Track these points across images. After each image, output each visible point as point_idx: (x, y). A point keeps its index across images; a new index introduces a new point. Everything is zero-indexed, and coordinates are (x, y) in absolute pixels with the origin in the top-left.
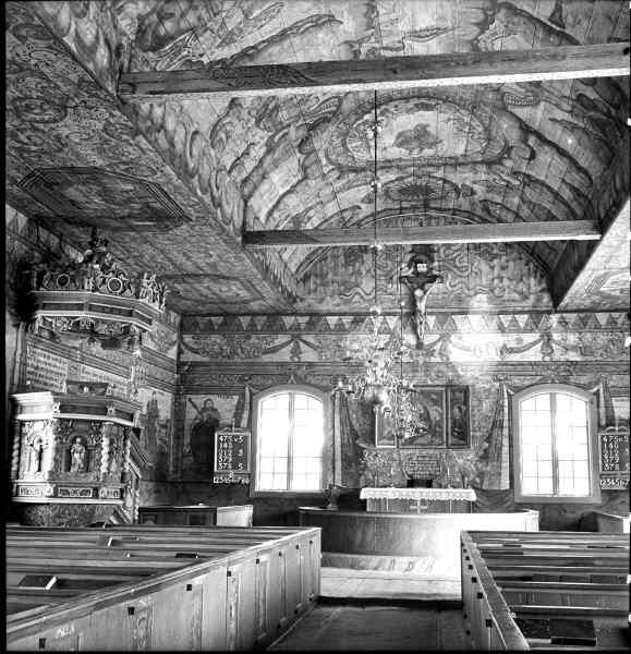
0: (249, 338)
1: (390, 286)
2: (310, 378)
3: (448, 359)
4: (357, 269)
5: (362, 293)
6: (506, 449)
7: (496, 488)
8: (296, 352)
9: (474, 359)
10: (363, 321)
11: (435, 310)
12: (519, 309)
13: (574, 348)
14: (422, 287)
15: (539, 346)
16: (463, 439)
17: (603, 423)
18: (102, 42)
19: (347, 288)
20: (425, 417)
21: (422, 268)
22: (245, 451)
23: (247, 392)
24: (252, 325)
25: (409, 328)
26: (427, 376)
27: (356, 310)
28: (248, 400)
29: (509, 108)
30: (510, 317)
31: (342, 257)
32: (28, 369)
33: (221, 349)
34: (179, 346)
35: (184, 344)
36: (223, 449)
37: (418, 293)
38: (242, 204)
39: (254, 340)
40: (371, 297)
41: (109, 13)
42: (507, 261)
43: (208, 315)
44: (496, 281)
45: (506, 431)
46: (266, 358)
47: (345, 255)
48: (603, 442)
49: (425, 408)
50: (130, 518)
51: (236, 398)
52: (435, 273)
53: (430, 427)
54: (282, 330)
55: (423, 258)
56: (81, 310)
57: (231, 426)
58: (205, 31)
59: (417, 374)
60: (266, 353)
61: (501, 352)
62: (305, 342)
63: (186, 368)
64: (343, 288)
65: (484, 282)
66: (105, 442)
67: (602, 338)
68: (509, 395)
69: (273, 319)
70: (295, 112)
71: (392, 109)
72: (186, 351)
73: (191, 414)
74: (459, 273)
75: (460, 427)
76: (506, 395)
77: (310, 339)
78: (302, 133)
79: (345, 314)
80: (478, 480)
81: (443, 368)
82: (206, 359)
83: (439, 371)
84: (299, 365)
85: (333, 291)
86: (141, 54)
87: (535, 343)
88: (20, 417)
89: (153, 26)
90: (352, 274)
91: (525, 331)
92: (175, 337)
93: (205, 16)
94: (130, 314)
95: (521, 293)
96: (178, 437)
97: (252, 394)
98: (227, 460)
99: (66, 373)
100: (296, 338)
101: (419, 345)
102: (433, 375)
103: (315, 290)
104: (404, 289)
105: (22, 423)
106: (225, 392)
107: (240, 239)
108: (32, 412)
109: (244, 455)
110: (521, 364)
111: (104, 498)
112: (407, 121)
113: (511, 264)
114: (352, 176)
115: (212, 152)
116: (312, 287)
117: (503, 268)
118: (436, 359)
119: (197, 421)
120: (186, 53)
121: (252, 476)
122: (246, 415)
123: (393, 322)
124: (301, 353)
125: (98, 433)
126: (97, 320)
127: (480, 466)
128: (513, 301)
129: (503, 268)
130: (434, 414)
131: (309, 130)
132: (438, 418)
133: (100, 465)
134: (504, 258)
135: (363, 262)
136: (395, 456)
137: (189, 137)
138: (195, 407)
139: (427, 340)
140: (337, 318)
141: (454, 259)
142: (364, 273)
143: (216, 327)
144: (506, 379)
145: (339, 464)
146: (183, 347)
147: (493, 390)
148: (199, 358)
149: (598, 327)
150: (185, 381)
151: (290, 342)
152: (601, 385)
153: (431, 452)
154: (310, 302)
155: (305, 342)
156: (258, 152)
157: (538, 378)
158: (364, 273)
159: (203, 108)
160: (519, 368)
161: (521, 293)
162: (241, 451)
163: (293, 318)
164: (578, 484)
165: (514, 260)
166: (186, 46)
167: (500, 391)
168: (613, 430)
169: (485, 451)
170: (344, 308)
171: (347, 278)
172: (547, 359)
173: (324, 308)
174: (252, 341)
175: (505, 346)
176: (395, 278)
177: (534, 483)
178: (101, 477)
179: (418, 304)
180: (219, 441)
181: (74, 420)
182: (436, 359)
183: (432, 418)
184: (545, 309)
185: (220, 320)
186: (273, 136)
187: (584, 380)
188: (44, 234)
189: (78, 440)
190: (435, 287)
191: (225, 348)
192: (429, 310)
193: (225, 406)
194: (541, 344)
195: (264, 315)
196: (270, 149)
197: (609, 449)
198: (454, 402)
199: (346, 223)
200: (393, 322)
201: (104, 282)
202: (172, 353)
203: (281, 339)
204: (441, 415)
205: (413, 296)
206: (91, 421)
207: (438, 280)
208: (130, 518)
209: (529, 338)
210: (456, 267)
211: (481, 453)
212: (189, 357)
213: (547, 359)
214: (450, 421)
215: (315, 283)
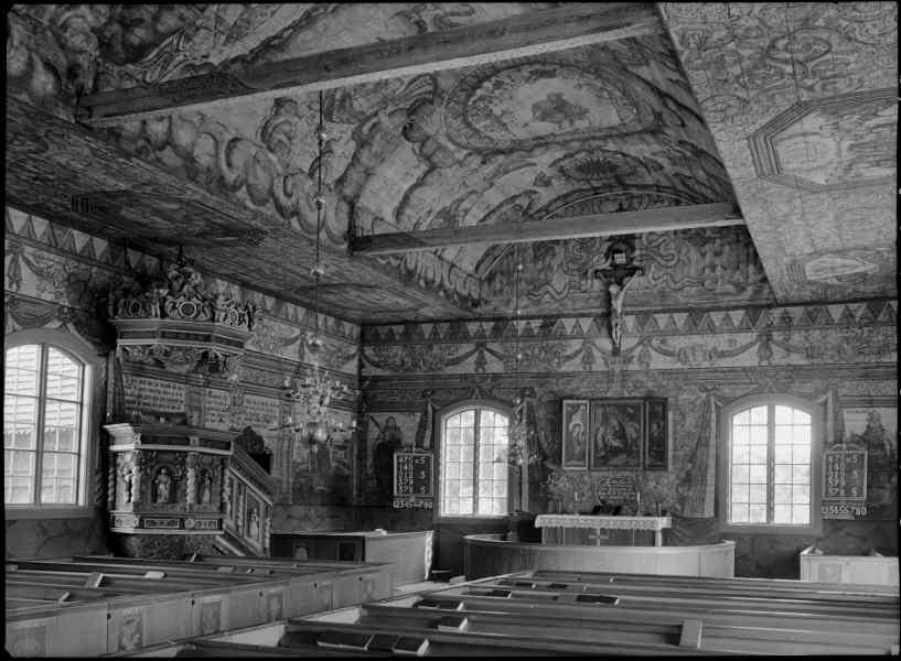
0: (430, 347)
1: (583, 282)
2: (495, 391)
3: (648, 365)
5: (553, 293)
6: (712, 471)
7: (699, 515)
8: (481, 363)
9: (679, 365)
10: (553, 324)
11: (634, 309)
12: (733, 303)
13: (797, 350)
14: (620, 283)
15: (756, 347)
16: (661, 460)
17: (831, 439)
18: (39, 66)
19: (537, 285)
20: (621, 434)
21: (620, 259)
22: (428, 474)
23: (430, 409)
24: (435, 333)
25: (604, 331)
26: (623, 387)
27: (545, 312)
28: (430, 419)
29: (630, 68)
30: (722, 315)
31: (531, 250)
32: (127, 398)
33: (403, 362)
34: (360, 360)
35: (366, 357)
36: (404, 471)
37: (613, 289)
38: (345, 207)
39: (436, 350)
40: (562, 296)
41: (49, 34)
42: (722, 245)
43: (387, 324)
44: (707, 271)
45: (712, 451)
46: (450, 370)
47: (534, 250)
48: (827, 463)
49: (620, 424)
50: (258, 546)
51: (419, 414)
52: (636, 263)
53: (626, 446)
54: (466, 338)
55: (623, 247)
56: (154, 337)
57: (411, 447)
58: (198, 29)
59: (611, 384)
60: (447, 365)
61: (711, 357)
62: (491, 351)
63: (367, 382)
64: (531, 287)
65: (693, 272)
66: (191, 473)
67: (834, 337)
68: (717, 406)
69: (455, 327)
70: (375, 99)
71: (508, 81)
72: (367, 364)
73: (374, 433)
74: (663, 262)
75: (659, 446)
76: (713, 406)
77: (495, 347)
78: (401, 119)
79: (533, 317)
80: (679, 507)
81: (641, 377)
82: (387, 373)
83: (638, 381)
84: (484, 377)
86: (116, 69)
87: (752, 344)
88: (115, 448)
89: (119, 37)
91: (739, 330)
92: (353, 350)
94: (207, 339)
95: (737, 285)
96: (361, 458)
97: (434, 411)
98: (408, 483)
99: (183, 398)
100: (481, 346)
101: (616, 352)
102: (630, 384)
103: (501, 291)
104: (597, 285)
105: (116, 454)
106: (409, 409)
107: (344, 246)
108: (121, 444)
109: (426, 476)
110: (732, 370)
111: (194, 529)
112: (542, 90)
113: (727, 248)
114: (501, 158)
115: (273, 158)
116: (498, 286)
117: (717, 254)
118: (634, 366)
119: (380, 441)
120: (181, 57)
121: (435, 500)
122: (428, 433)
123: (586, 324)
124: (486, 363)
125: (183, 463)
126: (172, 348)
127: (681, 490)
128: (727, 294)
129: (717, 254)
130: (630, 431)
131: (409, 115)
132: (634, 436)
133: (186, 495)
134: (718, 241)
135: (554, 255)
136: (586, 478)
137: (223, 148)
138: (377, 425)
139: (626, 344)
140: (524, 322)
141: (658, 246)
142: (555, 267)
143: (397, 337)
144: (714, 388)
145: (526, 487)
146: (364, 361)
147: (699, 402)
148: (379, 372)
149: (829, 322)
150: (366, 398)
151: (475, 350)
152: (830, 394)
153: (626, 474)
154: (496, 305)
155: (491, 351)
156: (344, 149)
157: (755, 386)
158: (555, 267)
159: (241, 113)
160: (730, 376)
161: (737, 285)
162: (423, 473)
163: (478, 324)
164: (795, 511)
165: (729, 244)
166: (178, 50)
167: (707, 404)
168: (841, 449)
169: (688, 473)
170: (532, 310)
171: (536, 275)
172: (764, 363)
173: (510, 312)
174: (434, 352)
175: (715, 348)
176: (590, 271)
177: (744, 510)
178: (188, 507)
179: (613, 302)
180: (398, 463)
181: (158, 451)
182: (634, 366)
183: (628, 436)
184: (764, 302)
185: (400, 329)
186: (359, 128)
187: (809, 388)
188: (134, 257)
189: (163, 471)
190: (634, 282)
191: (406, 360)
192: (628, 309)
193: (407, 425)
194: (756, 347)
195: (446, 321)
196: (363, 144)
197: (833, 470)
198: (653, 416)
199: (526, 212)
200: (586, 324)
201: (174, 307)
202: (351, 367)
203: (466, 348)
204: (637, 431)
205: (609, 294)
206: (174, 452)
207: (639, 272)
208: (258, 546)
209: (743, 339)
210: (661, 255)
211: (683, 475)
212: (370, 371)
213: (764, 363)
214: (647, 439)
215: (502, 283)
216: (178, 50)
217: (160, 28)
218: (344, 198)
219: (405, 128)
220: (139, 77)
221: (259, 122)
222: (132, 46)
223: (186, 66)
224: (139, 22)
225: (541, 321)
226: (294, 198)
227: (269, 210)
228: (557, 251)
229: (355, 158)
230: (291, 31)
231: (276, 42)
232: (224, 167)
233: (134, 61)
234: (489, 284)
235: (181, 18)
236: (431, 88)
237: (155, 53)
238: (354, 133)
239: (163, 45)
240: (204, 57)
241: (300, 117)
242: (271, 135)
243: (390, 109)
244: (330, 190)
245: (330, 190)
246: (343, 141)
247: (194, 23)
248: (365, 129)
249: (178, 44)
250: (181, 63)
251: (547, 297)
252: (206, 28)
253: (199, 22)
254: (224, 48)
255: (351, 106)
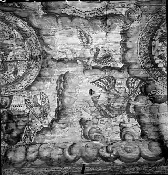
58: (31, 121)
86: (15, 146)
89: (10, 137)
93: (25, 119)
120: (33, 132)
166: (30, 130)
216: (30, 130)
217: (20, 128)
218: (153, 140)
219: (151, 100)
220: (24, 144)
221: (80, 134)
222: (15, 137)
223: (37, 133)
224: (13, 130)
226: (115, 153)
227: (99, 161)
229: (142, 125)
230: (60, 103)
231: (60, 109)
232: (68, 155)
233: (19, 141)
235: (24, 122)
236: (138, 81)
237: (24, 134)
238: (128, 116)
239: (24, 132)
240: (41, 127)
241: (97, 124)
242: (89, 136)
243: (133, 99)
244: (141, 141)
245: (141, 141)
246: (127, 121)
247: (29, 120)
248: (131, 110)
249: (29, 129)
250: (34, 133)
252: (33, 119)
253: (30, 119)
254: (45, 121)
255: (114, 108)
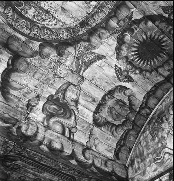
4: (160, 136)
47: (151, 134)
64: (155, 155)
85: (150, 161)
90: (158, 142)
142: (166, 136)
158: (166, 136)
170: (161, 170)
215: (138, 162)
225: (168, 174)
228: (163, 127)
234: (132, 167)
251: (167, 155)
